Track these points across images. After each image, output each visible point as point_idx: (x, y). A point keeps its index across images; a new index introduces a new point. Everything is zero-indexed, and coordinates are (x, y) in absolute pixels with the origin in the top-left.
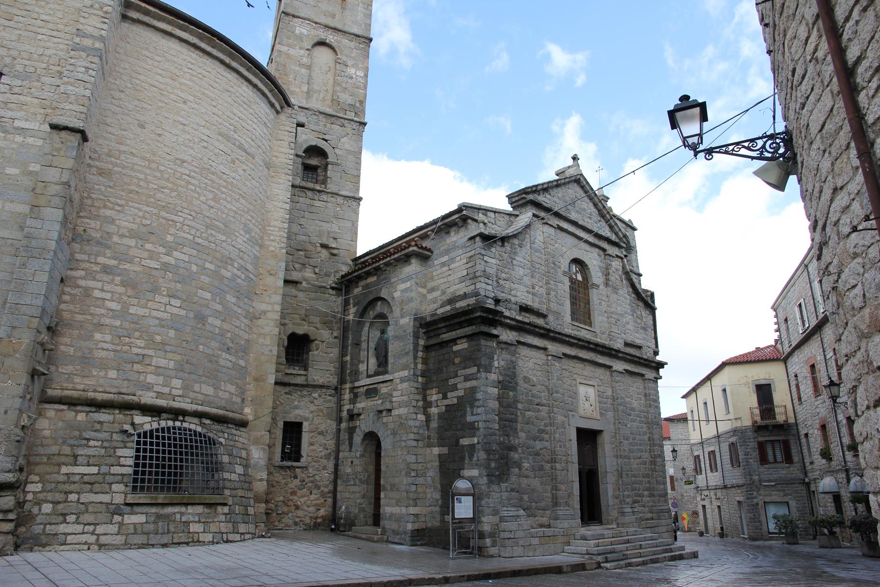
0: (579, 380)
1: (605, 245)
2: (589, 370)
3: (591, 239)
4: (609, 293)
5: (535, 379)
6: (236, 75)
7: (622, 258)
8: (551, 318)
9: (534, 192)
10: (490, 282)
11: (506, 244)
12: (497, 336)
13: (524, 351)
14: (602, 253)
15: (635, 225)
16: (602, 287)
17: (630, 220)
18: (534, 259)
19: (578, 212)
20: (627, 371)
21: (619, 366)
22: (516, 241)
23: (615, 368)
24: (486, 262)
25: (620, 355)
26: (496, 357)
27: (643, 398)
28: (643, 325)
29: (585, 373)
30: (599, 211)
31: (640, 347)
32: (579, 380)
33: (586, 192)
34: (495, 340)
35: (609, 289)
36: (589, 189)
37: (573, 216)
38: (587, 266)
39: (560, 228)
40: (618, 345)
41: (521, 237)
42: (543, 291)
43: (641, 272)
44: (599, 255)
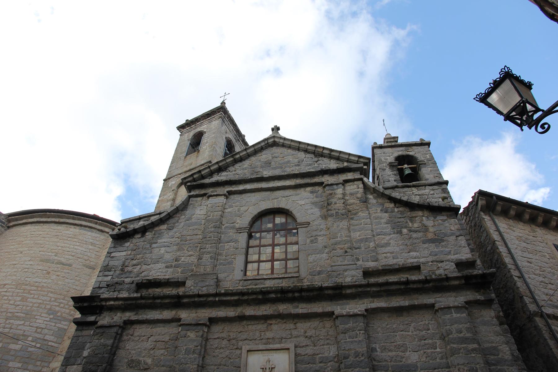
0: (245, 348)
1: (327, 179)
2: (277, 329)
3: (299, 181)
4: (330, 224)
5: (149, 361)
6: (65, 225)
7: (361, 179)
8: (189, 283)
9: (203, 177)
10: (111, 273)
11: (147, 234)
12: (95, 323)
13: (140, 331)
14: (319, 189)
15: (427, 140)
16: (318, 223)
17: (421, 140)
18: (185, 233)
19: (275, 168)
20: (370, 313)
21: (357, 307)
22: (164, 227)
23: (336, 313)
24: (113, 257)
25: (349, 291)
26: (88, 345)
27: (438, 342)
28: (430, 236)
29: (269, 335)
30: (314, 153)
31: (417, 268)
32: (245, 348)
33: (290, 147)
34: (94, 327)
35: (329, 219)
36: (289, 143)
37: (266, 173)
38: (288, 210)
39: (230, 193)
40: (352, 276)
41: (171, 221)
42: (194, 259)
43: (445, 179)
44: (312, 192)
